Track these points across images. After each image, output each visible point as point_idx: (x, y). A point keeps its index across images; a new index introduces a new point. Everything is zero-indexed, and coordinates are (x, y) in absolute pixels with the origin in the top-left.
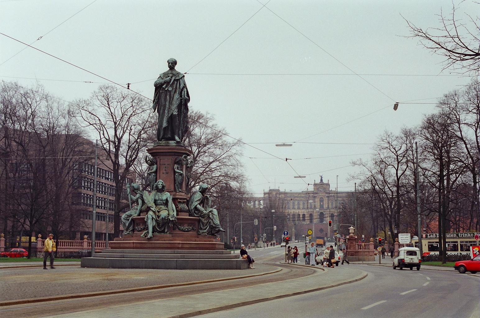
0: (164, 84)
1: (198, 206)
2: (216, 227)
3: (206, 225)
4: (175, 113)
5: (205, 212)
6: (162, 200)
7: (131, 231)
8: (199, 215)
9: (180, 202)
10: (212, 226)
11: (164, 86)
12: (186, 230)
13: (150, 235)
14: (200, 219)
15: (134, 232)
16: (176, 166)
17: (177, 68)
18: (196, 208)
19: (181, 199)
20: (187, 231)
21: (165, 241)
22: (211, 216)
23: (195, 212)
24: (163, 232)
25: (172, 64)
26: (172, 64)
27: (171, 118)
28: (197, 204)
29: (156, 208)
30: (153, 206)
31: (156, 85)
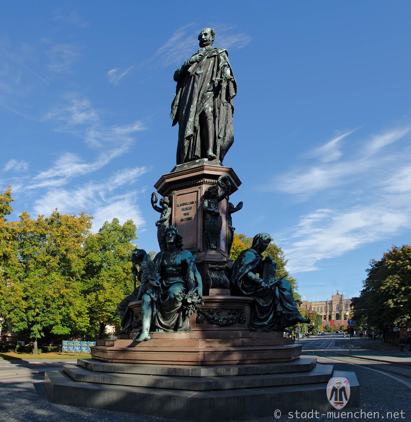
0: (190, 66)
1: (251, 274)
5: (263, 284)
6: (175, 266)
8: (251, 293)
9: (212, 270)
11: (190, 70)
12: (224, 323)
14: (255, 300)
18: (246, 278)
19: (213, 263)
20: (226, 325)
22: (277, 292)
23: (243, 287)
28: (247, 270)
29: (161, 281)
30: (156, 277)
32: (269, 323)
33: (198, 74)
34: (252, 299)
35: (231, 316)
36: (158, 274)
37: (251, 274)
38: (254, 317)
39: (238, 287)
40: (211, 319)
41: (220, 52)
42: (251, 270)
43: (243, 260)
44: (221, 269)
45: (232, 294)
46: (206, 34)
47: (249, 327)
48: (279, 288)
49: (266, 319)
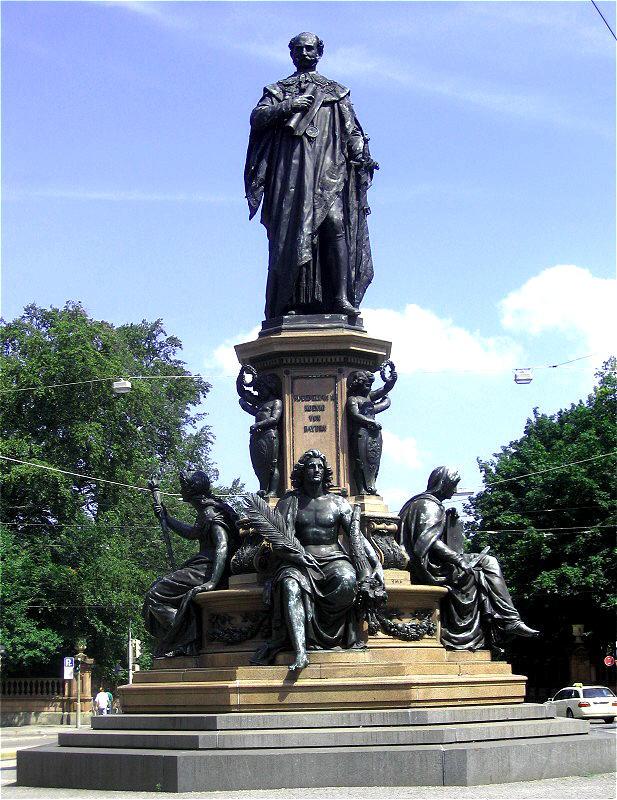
1: (440, 544)
2: (503, 622)
3: (472, 611)
4: (337, 214)
5: (463, 565)
6: (326, 525)
7: (190, 643)
10: (491, 616)
13: (302, 656)
15: (200, 647)
16: (357, 401)
17: (325, 68)
19: (381, 520)
21: (357, 675)
24: (346, 644)
25: (304, 56)
26: (304, 56)
27: (326, 232)
31: (257, 119)
32: (476, 634)
33: (309, 138)
34: (444, 589)
35: (416, 622)
36: (297, 542)
37: (440, 544)
38: (448, 622)
39: (422, 567)
40: (391, 627)
41: (342, 95)
42: (440, 538)
43: (423, 516)
44: (390, 532)
45: (413, 582)
46: (309, 48)
47: (442, 642)
48: (486, 572)
49: (468, 628)
